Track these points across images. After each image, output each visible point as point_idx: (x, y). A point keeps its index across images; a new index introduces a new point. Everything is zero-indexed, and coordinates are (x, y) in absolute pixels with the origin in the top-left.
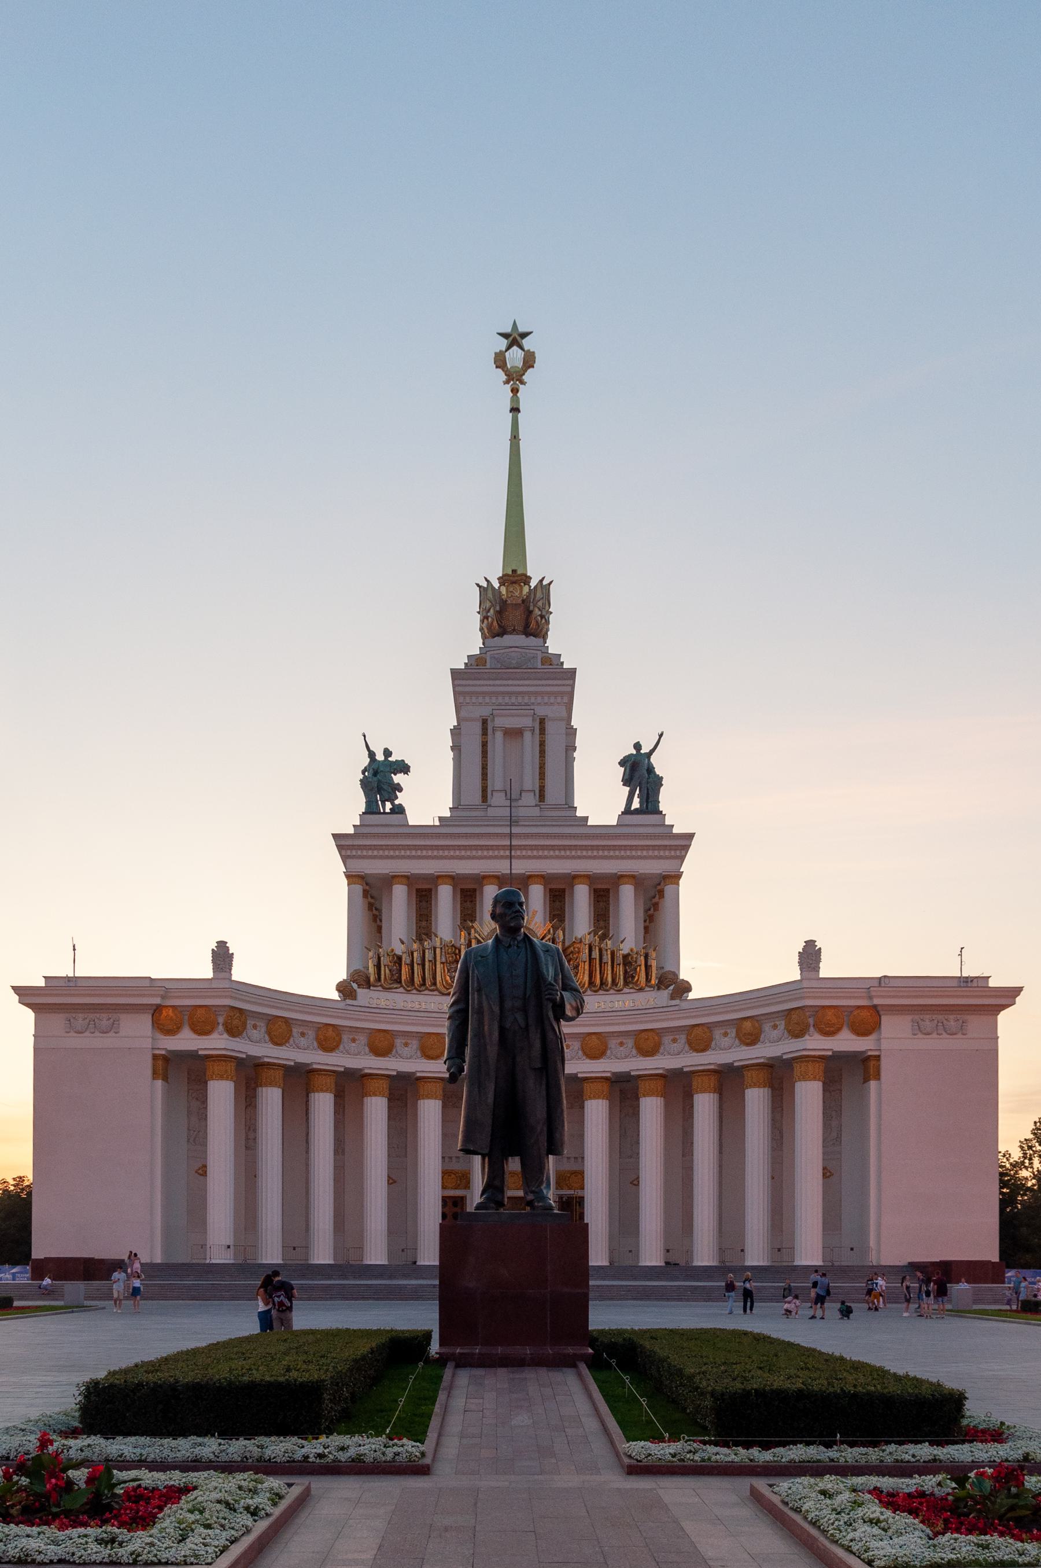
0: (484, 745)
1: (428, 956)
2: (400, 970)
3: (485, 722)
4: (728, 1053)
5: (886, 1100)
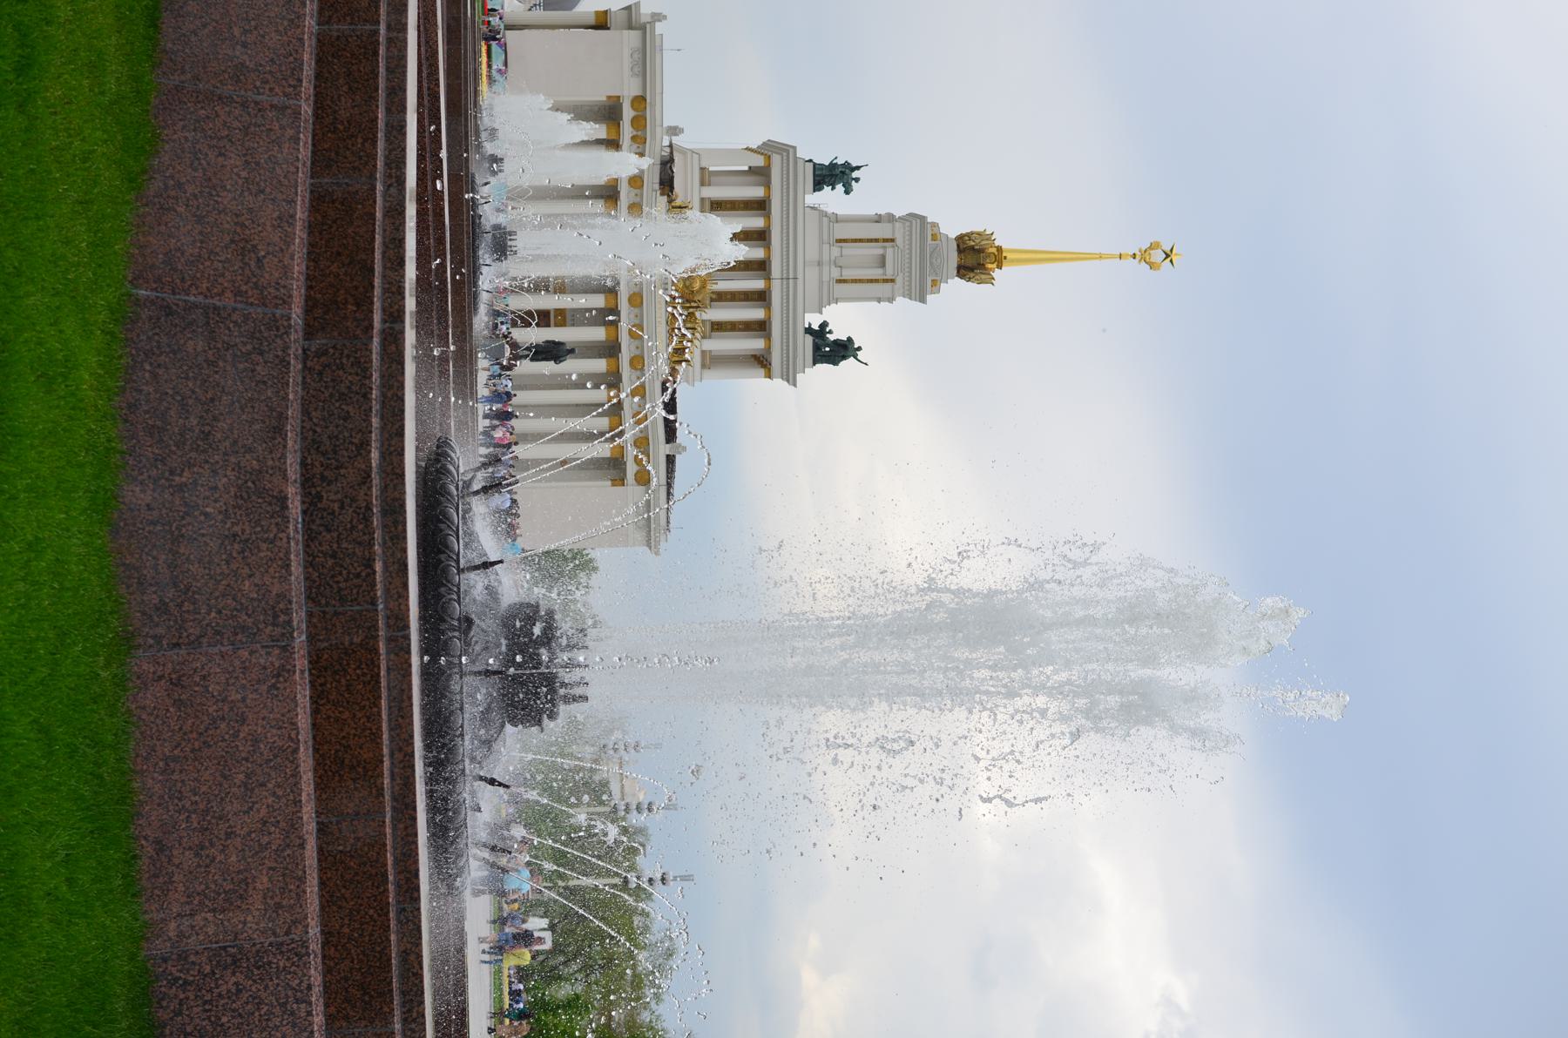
0: (876, 240)
3: (892, 240)
5: (602, 488)
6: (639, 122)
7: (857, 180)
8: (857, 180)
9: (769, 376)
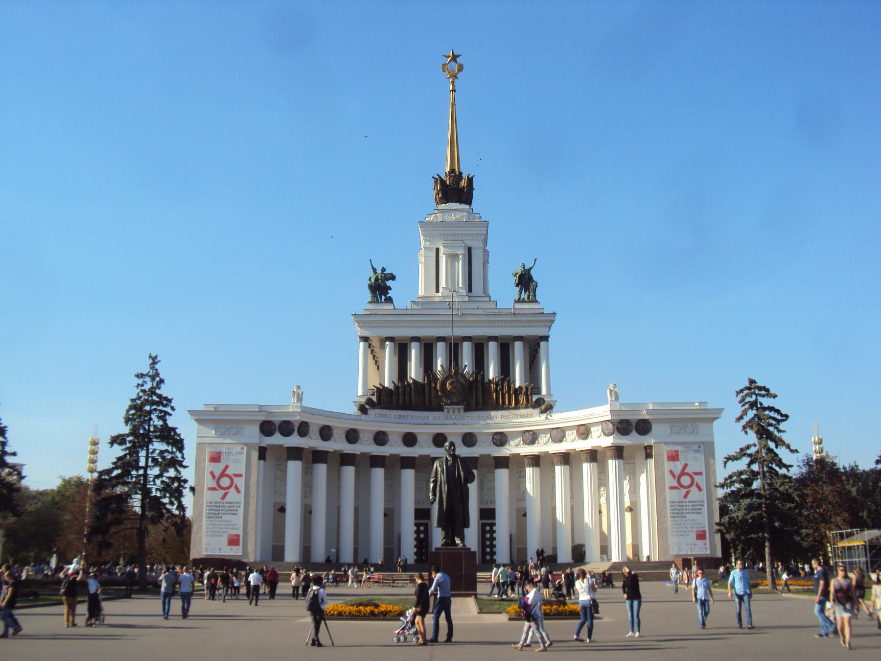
1: (407, 389)
2: (391, 398)
4: (572, 444)
6: (286, 428)
7: (383, 270)
8: (383, 270)
9: (546, 338)
